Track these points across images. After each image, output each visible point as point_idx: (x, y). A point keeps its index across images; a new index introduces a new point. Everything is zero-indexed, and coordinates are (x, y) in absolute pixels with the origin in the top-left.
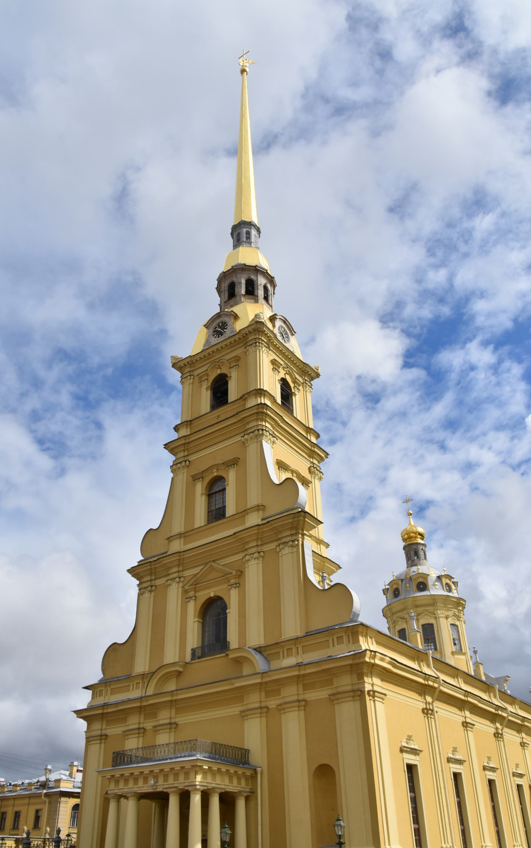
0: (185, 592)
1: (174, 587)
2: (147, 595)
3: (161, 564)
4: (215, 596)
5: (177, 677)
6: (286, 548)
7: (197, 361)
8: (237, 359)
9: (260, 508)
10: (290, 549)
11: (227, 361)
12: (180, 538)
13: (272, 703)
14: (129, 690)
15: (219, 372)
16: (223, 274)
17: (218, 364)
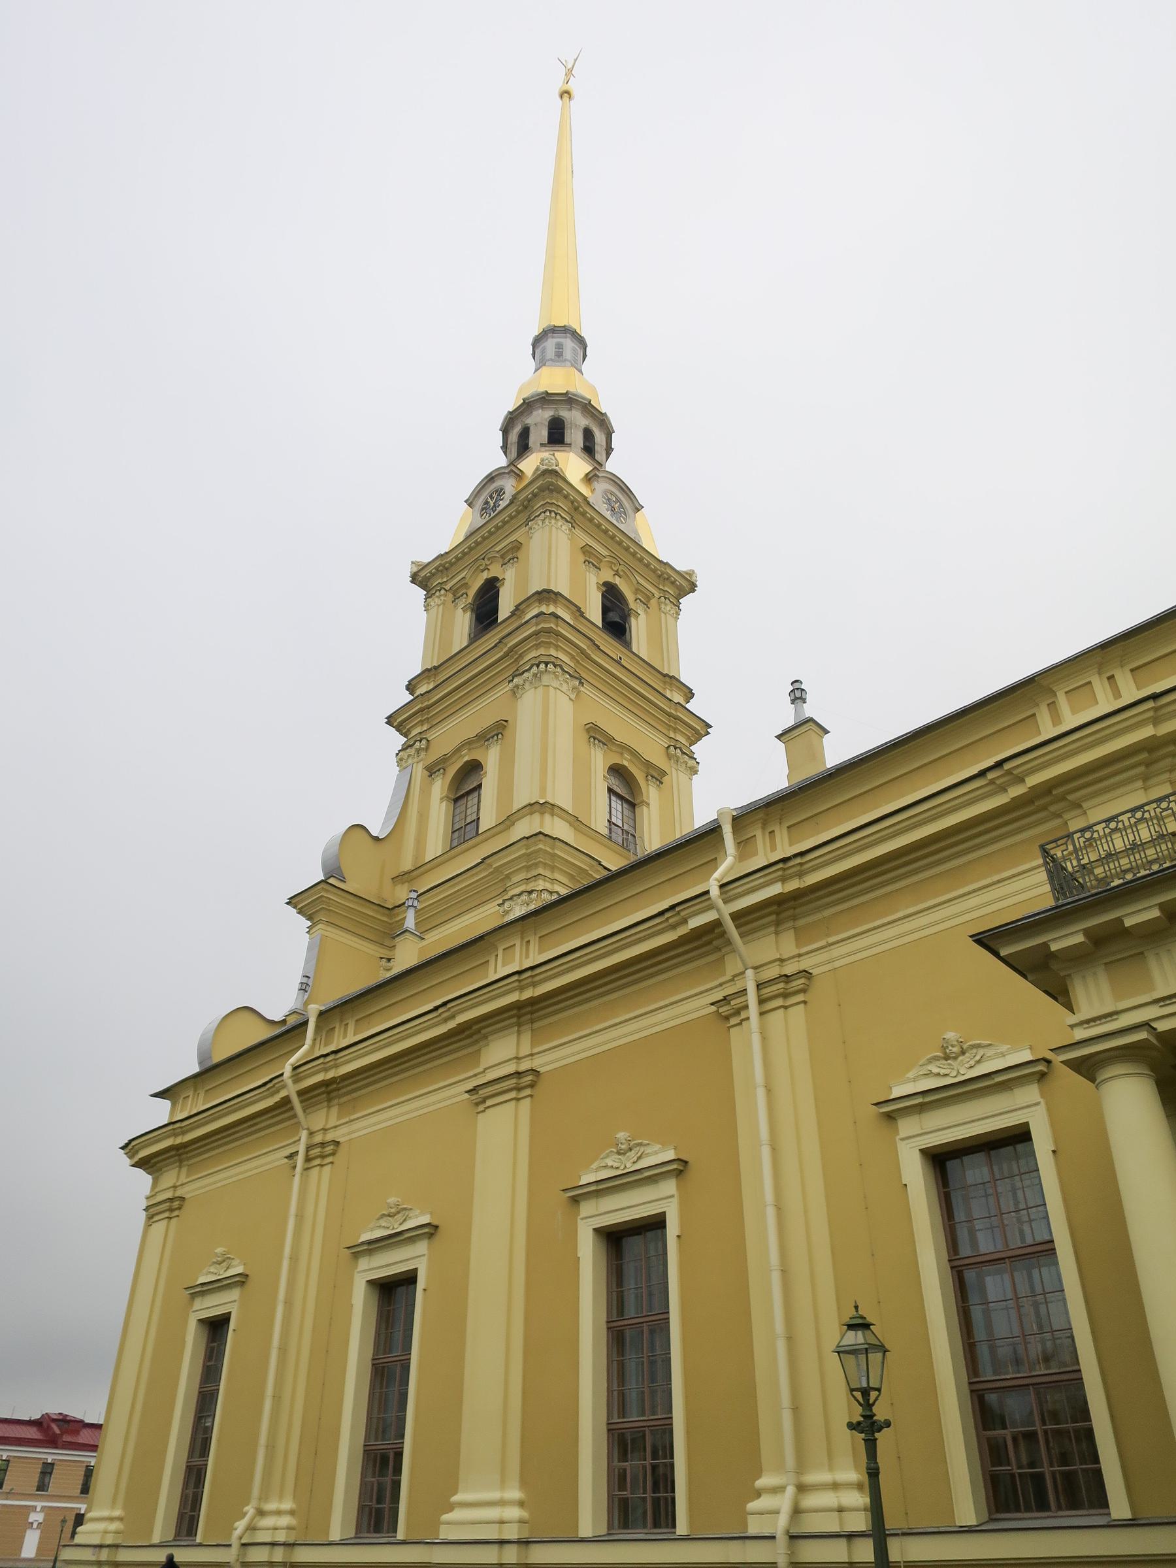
11: (638, 583)
12: (571, 825)
15: (617, 581)
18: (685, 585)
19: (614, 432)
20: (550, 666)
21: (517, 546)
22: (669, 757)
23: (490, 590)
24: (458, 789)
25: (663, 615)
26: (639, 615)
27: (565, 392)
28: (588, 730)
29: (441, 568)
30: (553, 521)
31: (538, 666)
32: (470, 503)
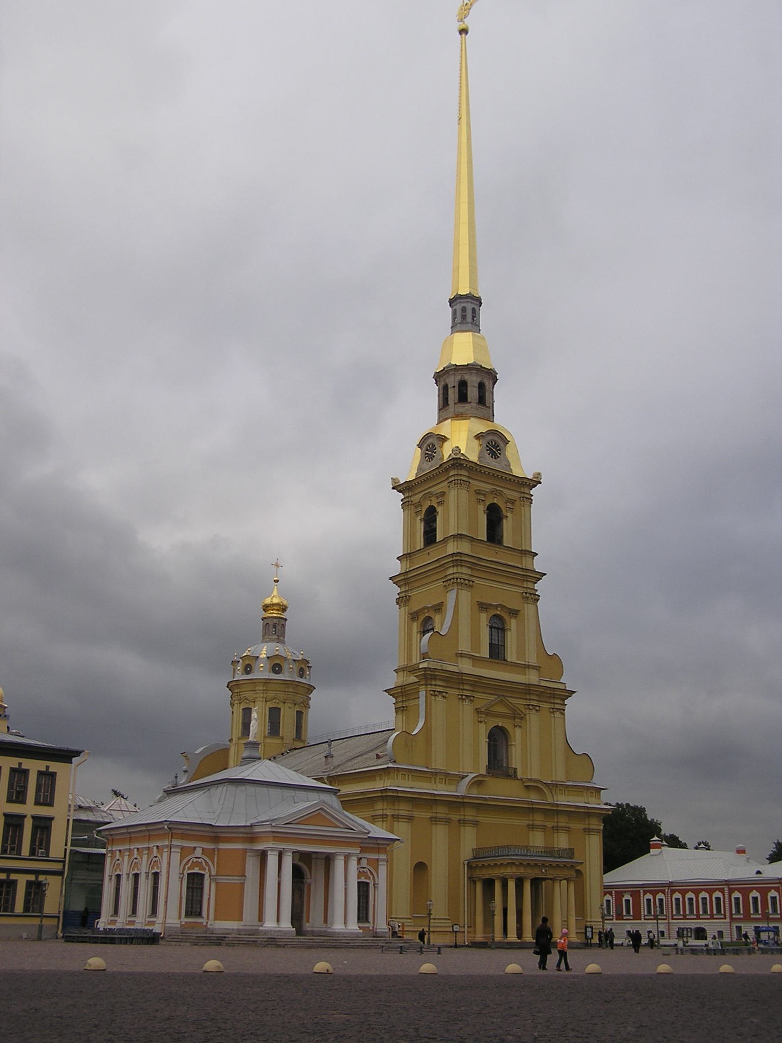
0: (478, 711)
1: (467, 703)
2: (440, 698)
3: (460, 677)
4: (502, 726)
5: (478, 785)
6: (558, 713)
7: (476, 470)
8: (513, 502)
9: (537, 668)
10: (560, 714)
11: (508, 498)
12: (470, 658)
13: (549, 824)
14: (431, 782)
15: (495, 502)
16: (479, 367)
17: (494, 493)
18: (535, 482)
19: (497, 374)
20: (459, 579)
21: (443, 494)
22: (523, 597)
23: (431, 512)
24: (424, 627)
25: (522, 507)
26: (507, 517)
27: (466, 364)
28: (478, 604)
29: (408, 488)
30: (459, 485)
31: (454, 579)
32: (420, 446)
